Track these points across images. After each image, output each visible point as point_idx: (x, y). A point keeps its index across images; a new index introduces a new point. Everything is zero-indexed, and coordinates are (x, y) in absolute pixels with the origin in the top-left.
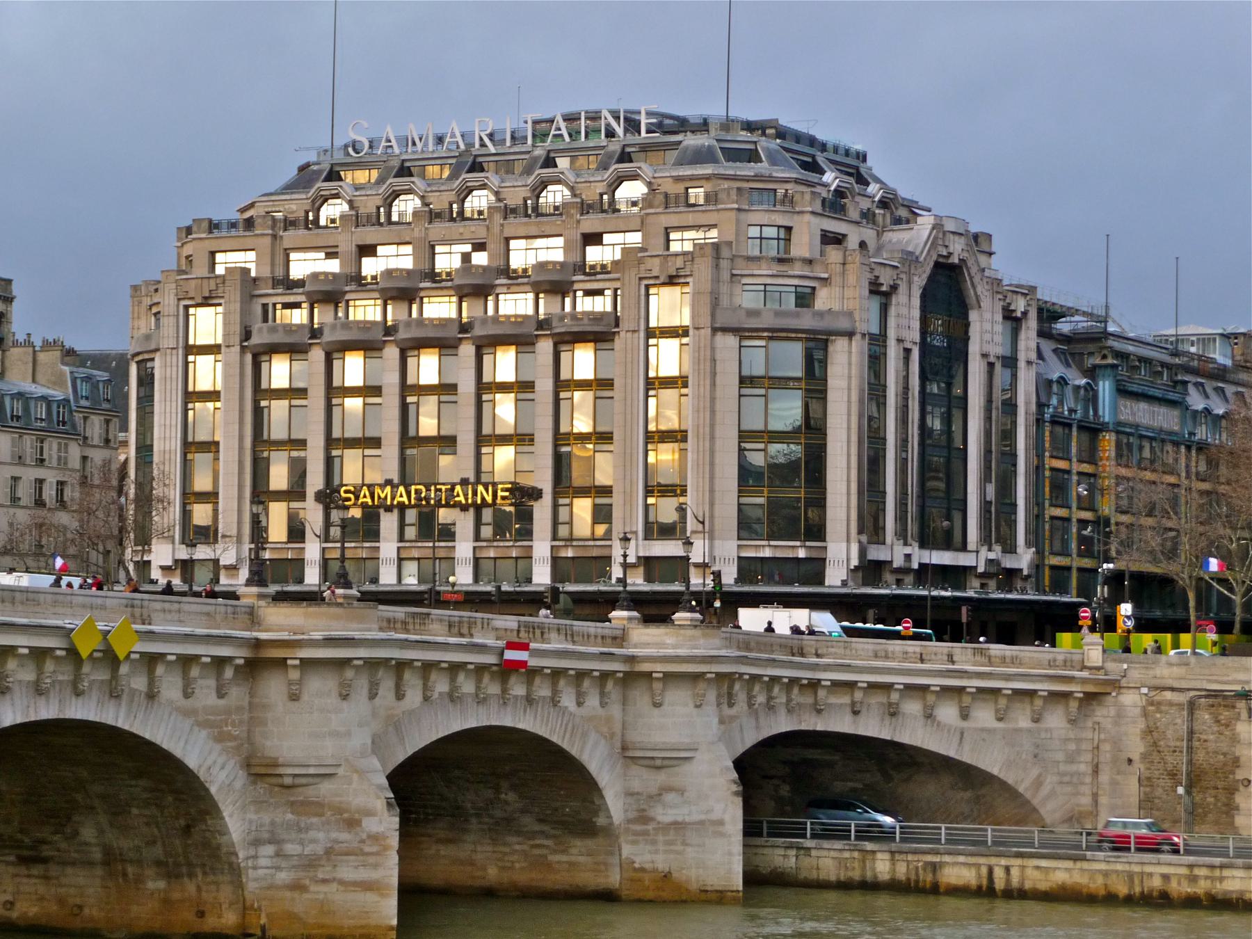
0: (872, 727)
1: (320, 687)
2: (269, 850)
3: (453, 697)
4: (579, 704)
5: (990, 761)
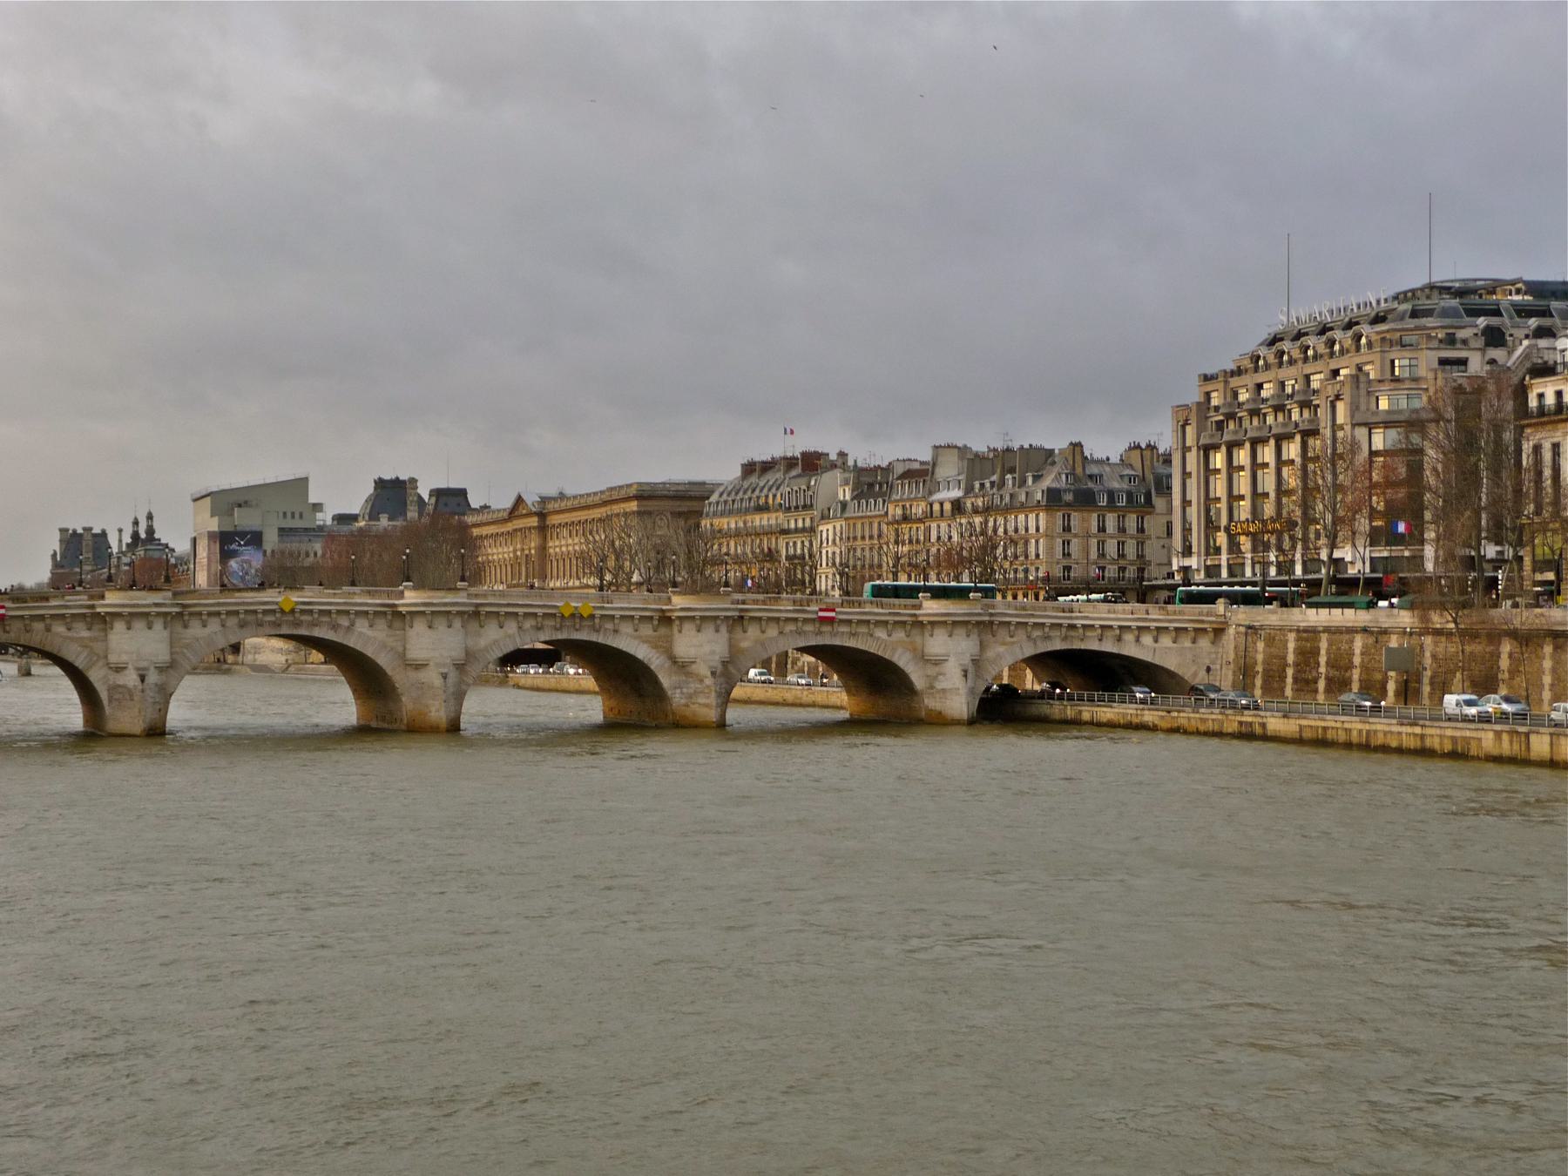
0: (1108, 646)
1: (689, 628)
2: (678, 691)
3: (799, 633)
4: (889, 635)
5: (1170, 663)
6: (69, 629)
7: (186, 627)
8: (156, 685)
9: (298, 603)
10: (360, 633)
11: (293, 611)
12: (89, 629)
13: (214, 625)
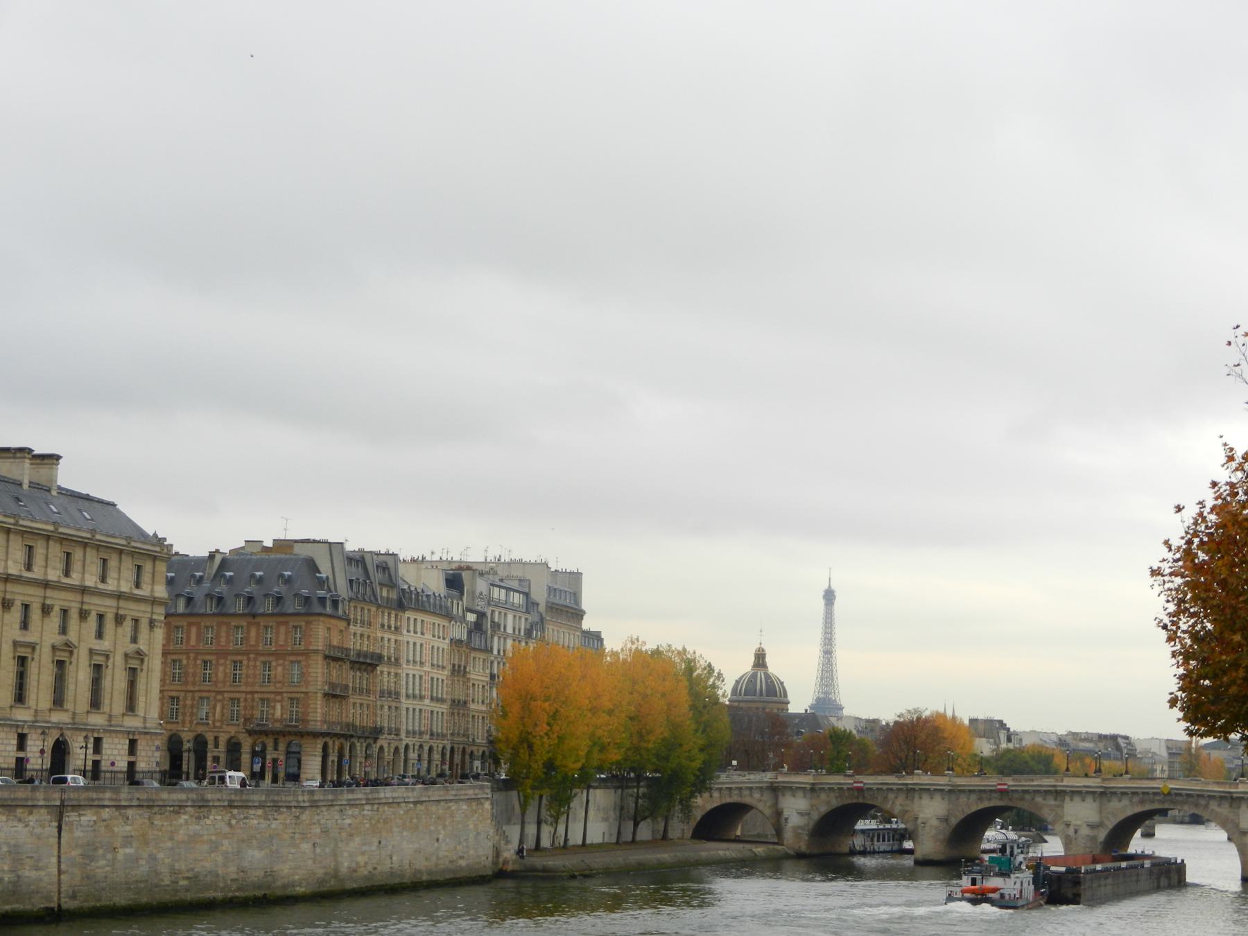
6: (1044, 799)
7: (1109, 801)
8: (1088, 836)
9: (1172, 789)
10: (1213, 810)
11: (1169, 794)
12: (1056, 800)
13: (1125, 802)
